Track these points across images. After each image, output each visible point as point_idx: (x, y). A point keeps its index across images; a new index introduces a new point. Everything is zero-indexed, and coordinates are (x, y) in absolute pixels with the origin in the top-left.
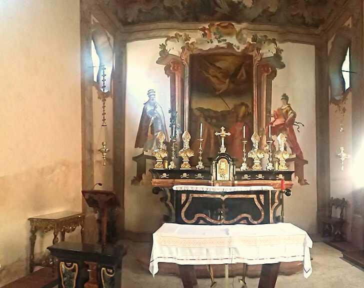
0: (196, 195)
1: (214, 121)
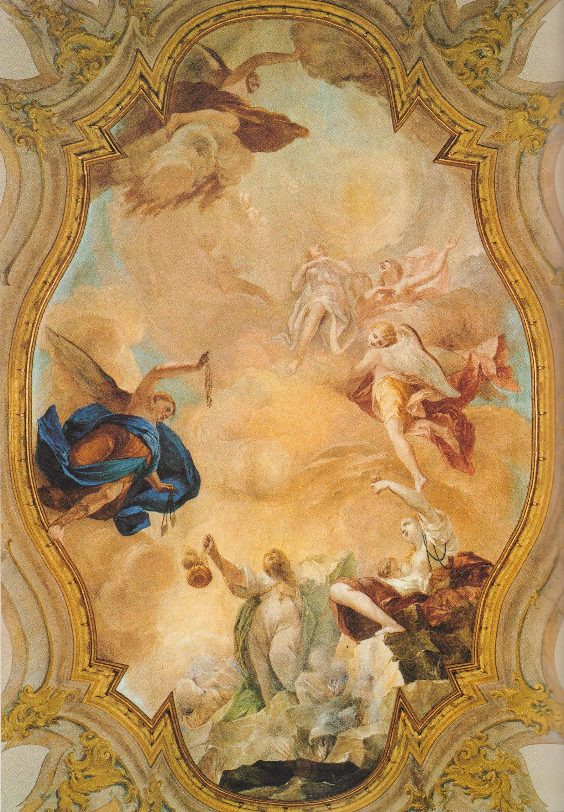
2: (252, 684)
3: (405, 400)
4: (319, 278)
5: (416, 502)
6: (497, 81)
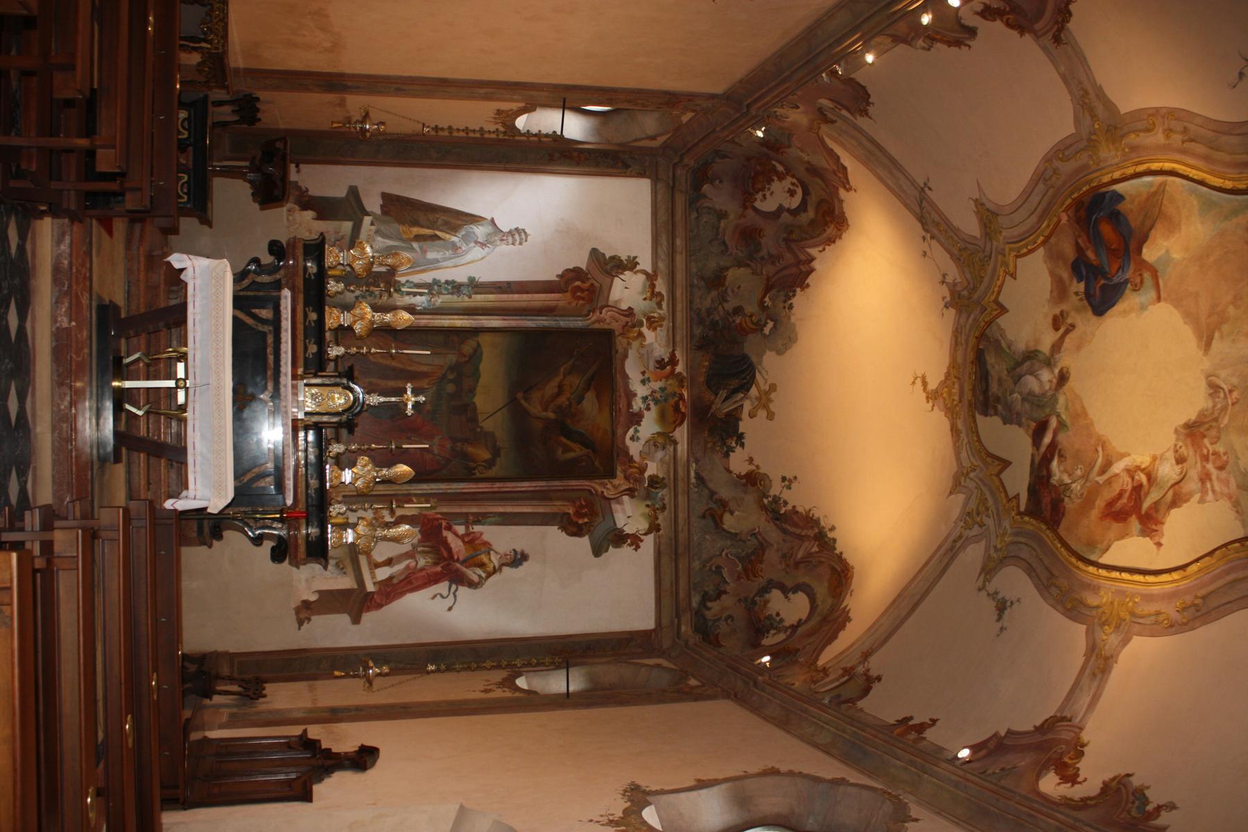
0: (270, 339)
1: (450, 388)
3: (1143, 470)
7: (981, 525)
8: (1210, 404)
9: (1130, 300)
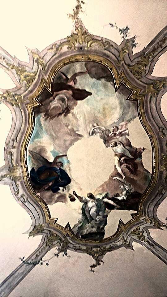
2: (86, 218)
3: (120, 159)
4: (97, 132)
5: (123, 181)
6: (145, 76)
7: (143, 232)
8: (98, 134)
9: (66, 168)
